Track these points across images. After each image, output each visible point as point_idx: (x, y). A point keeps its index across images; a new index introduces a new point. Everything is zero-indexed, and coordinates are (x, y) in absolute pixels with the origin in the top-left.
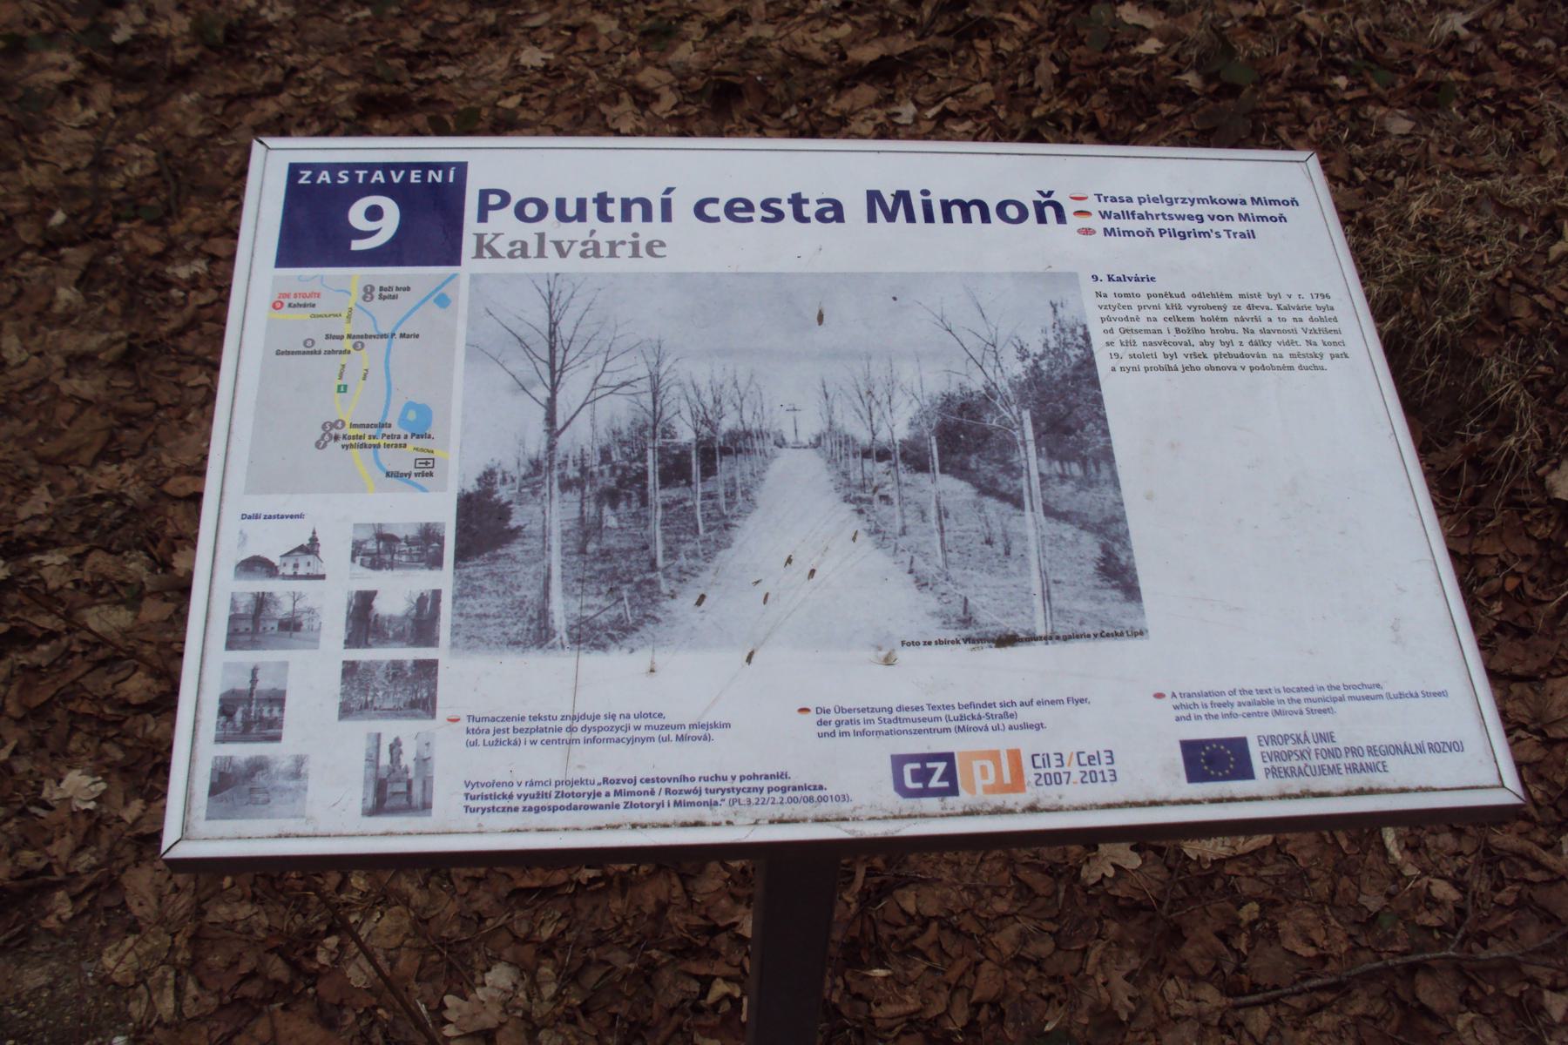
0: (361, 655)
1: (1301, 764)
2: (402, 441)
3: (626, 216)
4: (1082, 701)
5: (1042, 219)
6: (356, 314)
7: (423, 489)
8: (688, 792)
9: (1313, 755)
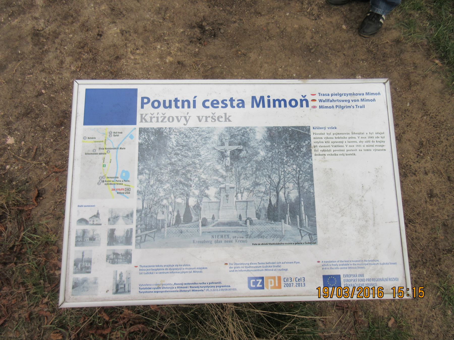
2: (121, 182)
3: (183, 107)
5: (302, 106)
7: (128, 198)
8: (196, 287)
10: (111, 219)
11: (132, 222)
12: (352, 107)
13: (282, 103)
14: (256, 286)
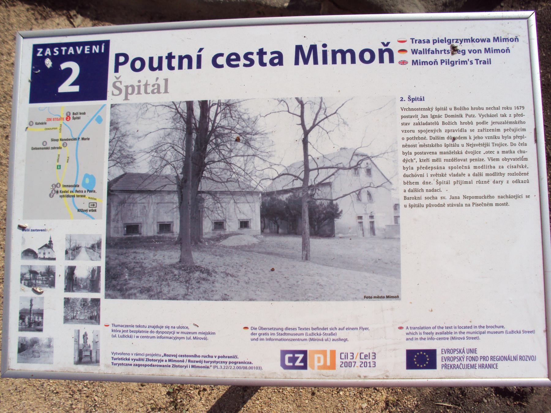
0: (71, 295)
1: (459, 363)
3: (180, 67)
4: (366, 329)
5: (381, 61)
6: (64, 127)
7: (93, 218)
8: (197, 362)
9: (465, 359)
10: (70, 252)
11: (100, 257)
12: (469, 63)
13: (348, 56)
14: (294, 364)
